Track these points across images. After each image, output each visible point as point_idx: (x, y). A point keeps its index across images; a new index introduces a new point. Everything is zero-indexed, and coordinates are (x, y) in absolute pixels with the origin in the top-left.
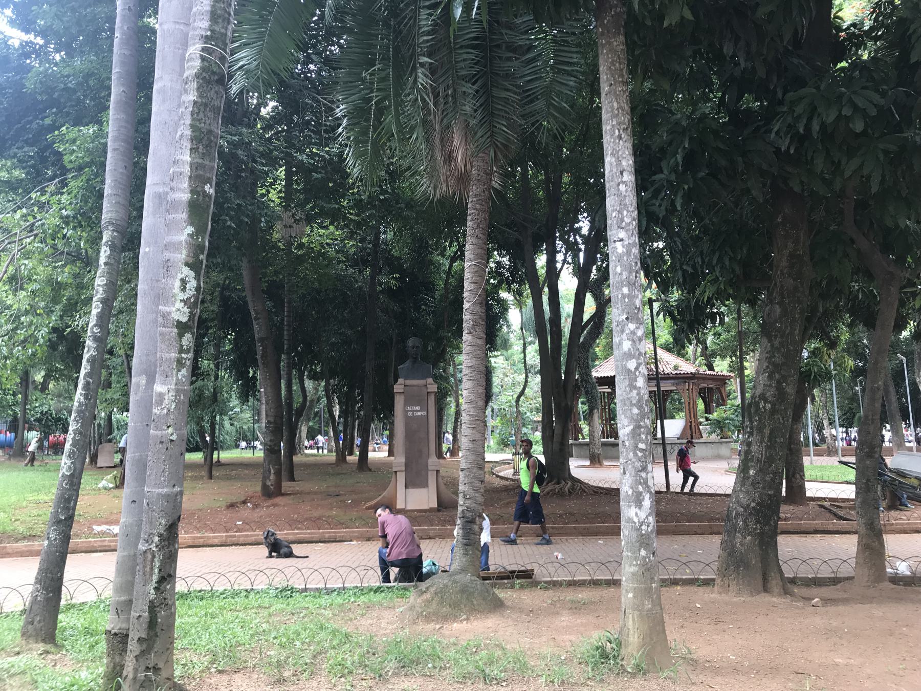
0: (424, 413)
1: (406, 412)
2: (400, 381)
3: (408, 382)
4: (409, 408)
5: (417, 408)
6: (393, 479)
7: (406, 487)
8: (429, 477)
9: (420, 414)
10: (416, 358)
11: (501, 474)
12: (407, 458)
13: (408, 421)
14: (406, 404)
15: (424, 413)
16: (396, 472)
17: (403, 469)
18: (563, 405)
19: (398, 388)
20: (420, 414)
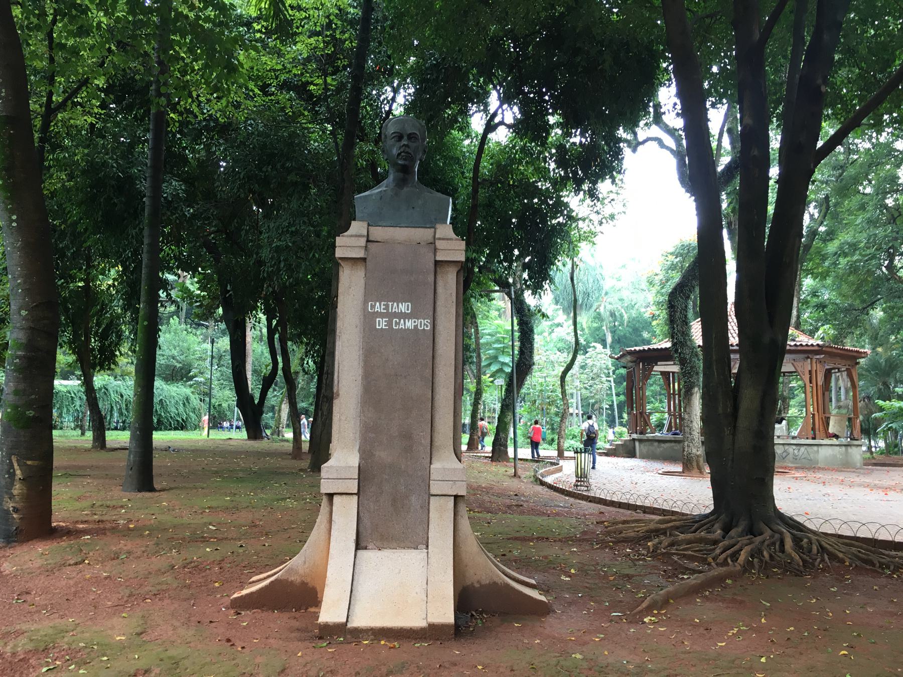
0: (424, 324)
1: (369, 318)
2: (357, 227)
3: (378, 233)
4: (379, 307)
5: (404, 307)
6: (322, 519)
7: (359, 545)
8: (433, 515)
9: (410, 324)
10: (405, 170)
11: (549, 480)
12: (366, 454)
13: (373, 342)
14: (370, 294)
15: (424, 324)
16: (331, 496)
17: (353, 487)
18: (766, 339)
19: (347, 245)
20: (410, 324)
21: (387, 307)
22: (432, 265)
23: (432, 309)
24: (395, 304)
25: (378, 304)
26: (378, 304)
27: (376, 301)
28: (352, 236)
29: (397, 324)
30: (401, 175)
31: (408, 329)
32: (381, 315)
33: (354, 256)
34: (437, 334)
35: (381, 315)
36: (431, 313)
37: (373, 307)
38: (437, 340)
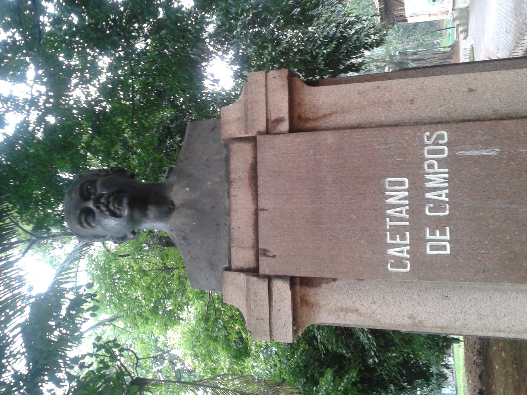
4: (399, 249)
5: (397, 194)
14: (372, 270)
20: (437, 178)
21: (398, 231)
22: (299, 138)
23: (397, 130)
24: (390, 212)
25: (391, 252)
26: (391, 252)
27: (386, 258)
28: (248, 307)
29: (438, 206)
30: (152, 211)
31: (449, 180)
32: (418, 242)
33: (288, 303)
34: (455, 115)
35: (418, 242)
36: (408, 131)
37: (399, 262)
38: (469, 114)
